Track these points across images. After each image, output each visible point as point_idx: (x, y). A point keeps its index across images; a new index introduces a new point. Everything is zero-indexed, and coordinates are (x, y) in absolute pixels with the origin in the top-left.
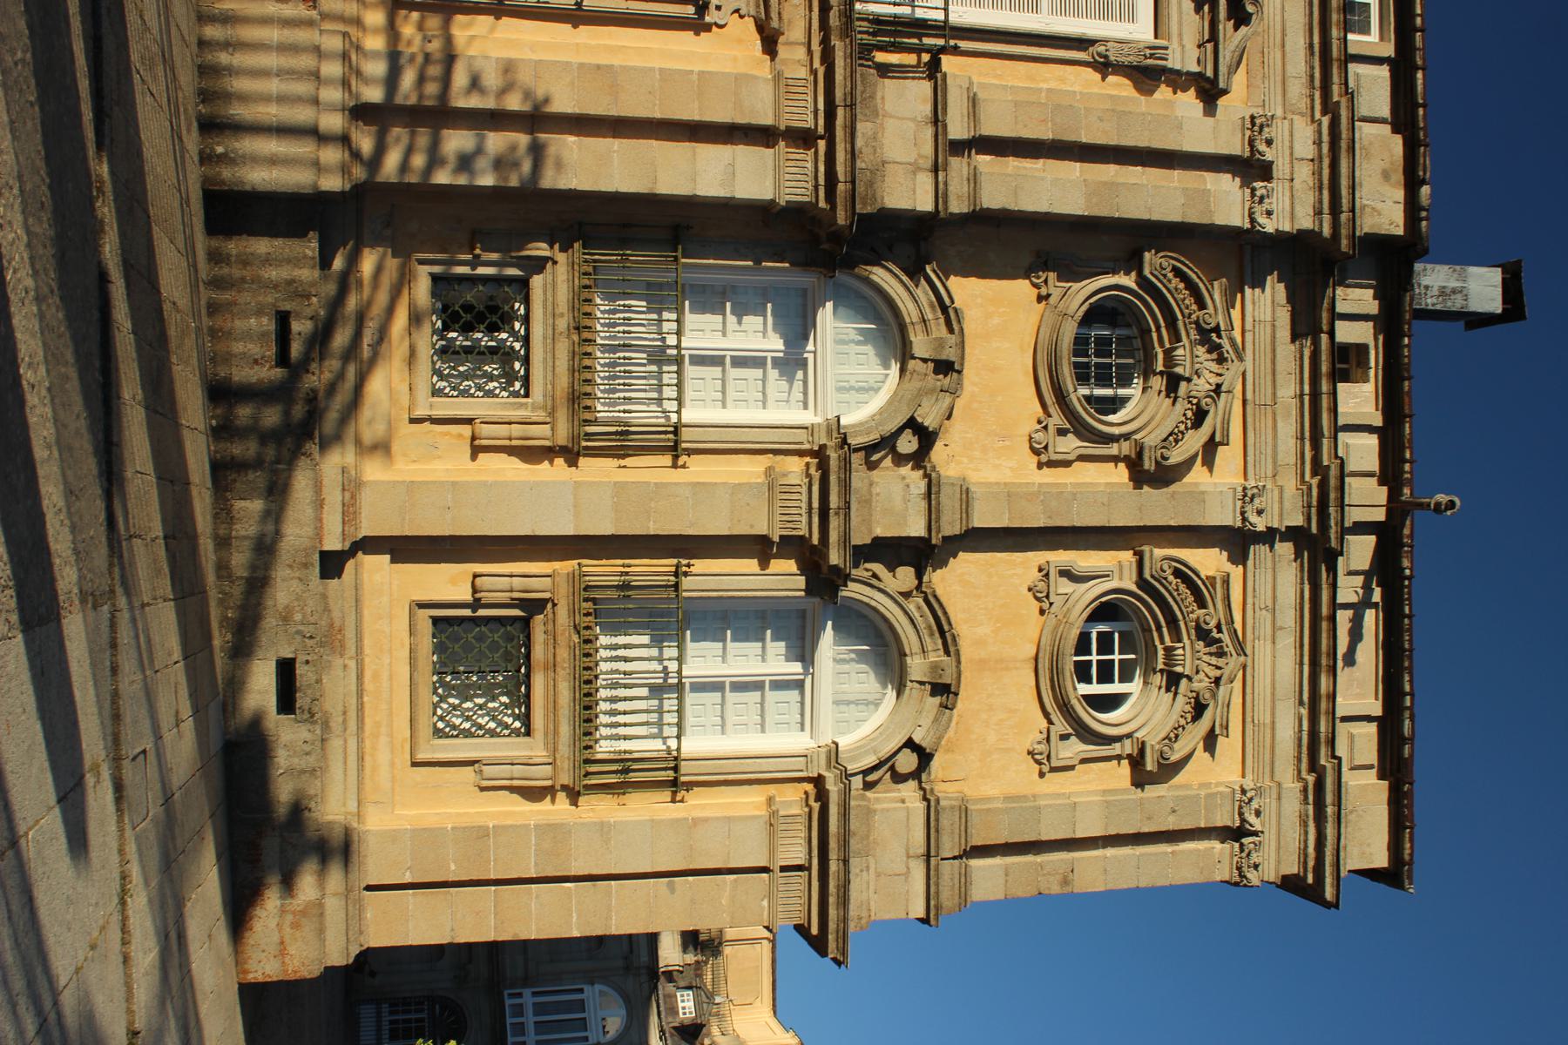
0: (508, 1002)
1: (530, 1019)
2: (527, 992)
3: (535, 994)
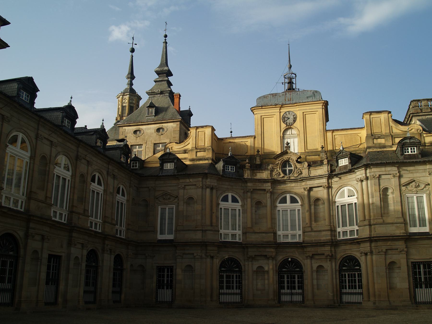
0: (342, 238)
1: (348, 228)
2: (339, 230)
3: (339, 227)
